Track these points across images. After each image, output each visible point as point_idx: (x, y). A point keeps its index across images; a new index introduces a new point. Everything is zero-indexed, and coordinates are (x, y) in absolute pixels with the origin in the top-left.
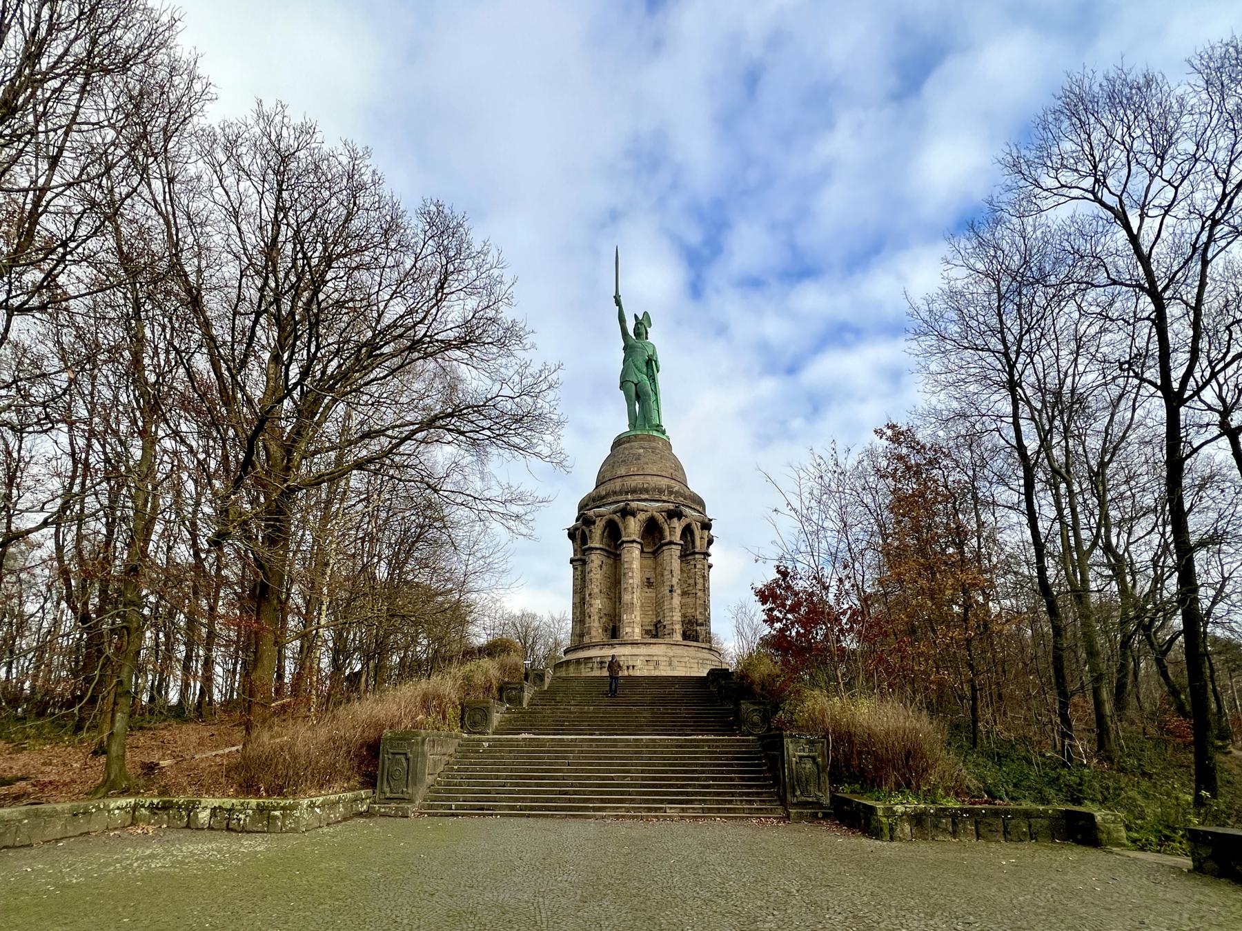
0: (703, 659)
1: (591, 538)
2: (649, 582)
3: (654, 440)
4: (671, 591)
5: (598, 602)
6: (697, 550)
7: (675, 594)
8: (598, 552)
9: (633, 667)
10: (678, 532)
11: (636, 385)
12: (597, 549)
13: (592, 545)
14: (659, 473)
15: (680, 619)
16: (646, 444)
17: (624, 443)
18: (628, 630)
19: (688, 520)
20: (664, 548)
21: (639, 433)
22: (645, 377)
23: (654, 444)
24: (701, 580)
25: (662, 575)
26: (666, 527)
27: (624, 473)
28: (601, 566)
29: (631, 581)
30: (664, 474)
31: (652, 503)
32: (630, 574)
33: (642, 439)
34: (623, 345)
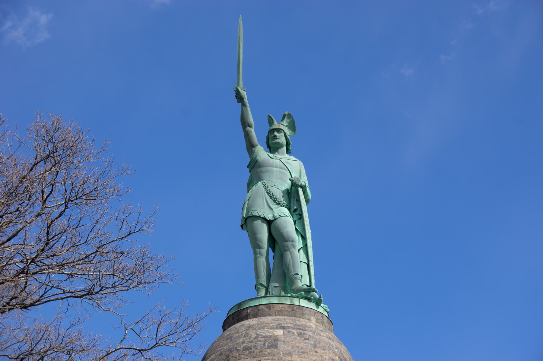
3: (302, 315)
11: (269, 223)
16: (288, 321)
17: (247, 317)
21: (274, 300)
22: (285, 211)
23: (302, 321)
33: (280, 313)
34: (248, 160)
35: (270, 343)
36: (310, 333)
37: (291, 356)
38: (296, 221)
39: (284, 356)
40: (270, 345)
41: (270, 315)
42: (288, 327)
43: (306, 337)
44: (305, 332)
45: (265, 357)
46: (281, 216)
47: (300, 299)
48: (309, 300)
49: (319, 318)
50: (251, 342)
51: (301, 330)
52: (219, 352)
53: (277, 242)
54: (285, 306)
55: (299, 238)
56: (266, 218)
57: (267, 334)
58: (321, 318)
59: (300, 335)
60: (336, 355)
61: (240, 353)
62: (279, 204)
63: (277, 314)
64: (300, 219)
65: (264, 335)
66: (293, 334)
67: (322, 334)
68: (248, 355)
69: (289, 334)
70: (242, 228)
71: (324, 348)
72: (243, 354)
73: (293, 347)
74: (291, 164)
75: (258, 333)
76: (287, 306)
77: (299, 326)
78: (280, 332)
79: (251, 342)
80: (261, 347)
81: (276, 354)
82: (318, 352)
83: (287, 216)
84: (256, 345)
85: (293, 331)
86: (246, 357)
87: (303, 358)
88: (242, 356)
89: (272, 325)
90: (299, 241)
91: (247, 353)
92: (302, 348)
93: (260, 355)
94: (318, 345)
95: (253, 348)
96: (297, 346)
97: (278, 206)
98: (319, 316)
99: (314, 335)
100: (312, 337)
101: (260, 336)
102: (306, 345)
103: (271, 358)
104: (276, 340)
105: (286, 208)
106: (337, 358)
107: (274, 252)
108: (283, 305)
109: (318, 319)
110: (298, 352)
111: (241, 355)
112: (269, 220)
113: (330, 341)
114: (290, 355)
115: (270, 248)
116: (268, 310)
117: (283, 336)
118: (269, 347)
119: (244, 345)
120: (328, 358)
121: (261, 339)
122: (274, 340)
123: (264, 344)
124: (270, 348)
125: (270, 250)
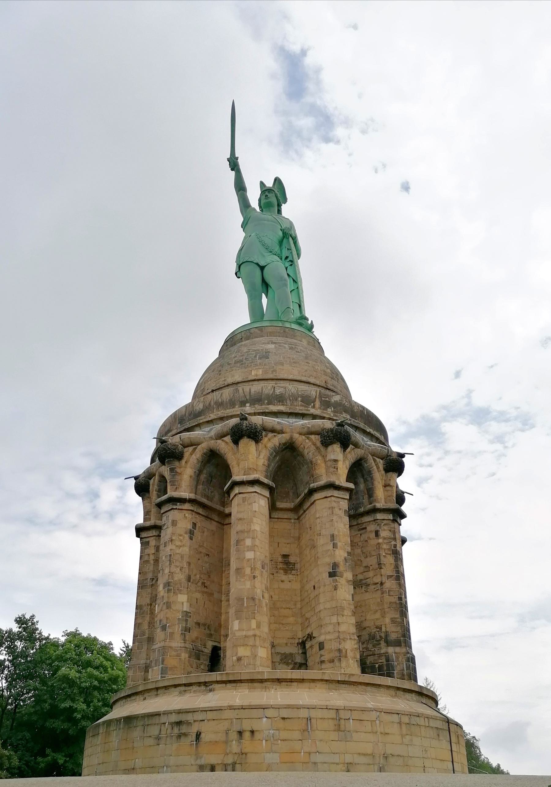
0: (410, 715)
1: (173, 483)
2: (287, 563)
3: (294, 337)
4: (332, 574)
5: (183, 598)
6: (379, 505)
7: (342, 581)
8: (187, 506)
9: (252, 732)
10: (343, 469)
11: (262, 268)
12: (182, 501)
13: (176, 494)
14: (304, 379)
15: (353, 630)
18: (242, 652)
19: (359, 452)
20: (317, 496)
24: (390, 559)
25: (314, 547)
26: (319, 460)
27: (238, 378)
28: (191, 533)
29: (250, 555)
30: (312, 380)
31: (292, 420)
32: (248, 542)
33: (271, 334)
35: (261, 355)
36: (301, 348)
37: (283, 365)
38: (287, 267)
39: (275, 365)
40: (261, 356)
41: (262, 336)
42: (279, 343)
43: (297, 351)
44: (297, 347)
45: (256, 367)
46: (273, 261)
47: (292, 324)
48: (300, 324)
49: (310, 341)
50: (242, 356)
51: (292, 345)
52: (212, 370)
53: (270, 287)
54: (277, 328)
55: (290, 282)
56: (259, 263)
57: (258, 348)
58: (313, 342)
59: (291, 348)
60: (328, 368)
61: (232, 366)
62: (271, 252)
63: (268, 335)
64: (291, 265)
65: (256, 349)
66: (285, 347)
67: (314, 351)
68: (239, 367)
69: (280, 347)
70: (236, 275)
71: (316, 360)
72: (234, 367)
73: (284, 358)
74: (282, 220)
75: (249, 348)
76: (278, 328)
77: (290, 342)
78: (273, 346)
79: (242, 356)
80: (252, 359)
81: (267, 364)
82: (309, 363)
83: (278, 261)
84: (247, 357)
85: (284, 345)
86: (238, 369)
87: (294, 367)
88: (234, 368)
89: (263, 341)
90: (290, 285)
91: (238, 365)
92: (293, 359)
93: (251, 366)
94: (310, 358)
95: (244, 360)
96: (288, 357)
97: (271, 253)
98: (310, 339)
99: (305, 350)
100: (304, 351)
101: (251, 351)
102: (297, 356)
103: (262, 367)
104: (267, 352)
105: (278, 257)
106: (329, 370)
107: (267, 298)
108: (275, 327)
109: (310, 342)
110: (290, 362)
111: (232, 367)
112: (261, 265)
113: (321, 356)
114: (282, 364)
115: (263, 294)
116: (260, 332)
117: (274, 349)
118: (260, 358)
119: (235, 359)
120: (319, 369)
121: (253, 353)
122: (265, 352)
123: (256, 356)
124: (261, 359)
125: (263, 295)
